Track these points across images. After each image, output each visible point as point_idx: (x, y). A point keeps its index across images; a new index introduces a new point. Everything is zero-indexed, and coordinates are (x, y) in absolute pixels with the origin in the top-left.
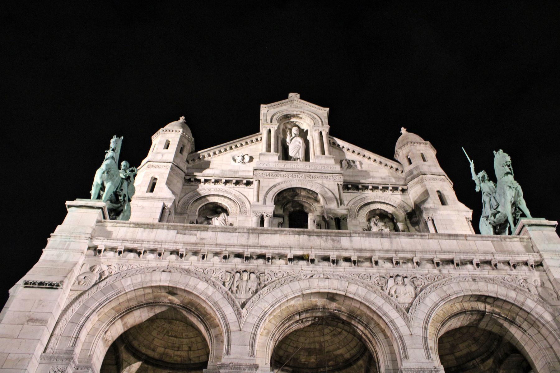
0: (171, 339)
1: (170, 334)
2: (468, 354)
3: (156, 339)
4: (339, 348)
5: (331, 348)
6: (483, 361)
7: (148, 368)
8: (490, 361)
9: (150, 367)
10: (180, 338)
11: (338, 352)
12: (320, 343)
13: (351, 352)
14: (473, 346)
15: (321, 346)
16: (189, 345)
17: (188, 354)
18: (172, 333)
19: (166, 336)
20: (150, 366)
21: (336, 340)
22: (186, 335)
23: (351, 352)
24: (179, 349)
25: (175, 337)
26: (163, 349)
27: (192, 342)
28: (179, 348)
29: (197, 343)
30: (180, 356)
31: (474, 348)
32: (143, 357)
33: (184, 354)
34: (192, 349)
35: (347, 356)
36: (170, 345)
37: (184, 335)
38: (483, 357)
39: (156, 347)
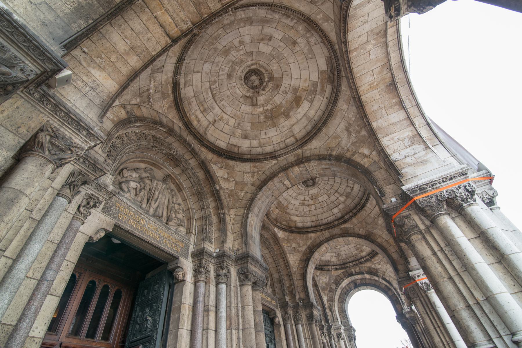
0: (208, 94)
1: (213, 87)
2: (328, 261)
3: (200, 74)
4: (297, 216)
5: (292, 212)
6: (336, 269)
7: (168, 96)
8: (340, 272)
9: (171, 98)
10: (216, 102)
11: (294, 218)
12: (289, 203)
13: (305, 223)
14: (334, 258)
15: (287, 206)
16: (217, 119)
17: (208, 127)
18: (216, 88)
19: (209, 84)
20: (172, 96)
21: (301, 208)
22: (223, 105)
23: (305, 223)
24: (204, 111)
25: (214, 96)
26: (192, 94)
27: (222, 117)
28: (205, 110)
29: (227, 123)
30: (199, 121)
31: (334, 259)
32: (178, 76)
33: (205, 123)
34: (216, 125)
35: (300, 225)
36: (201, 97)
37: (222, 102)
38: (338, 267)
39: (191, 83)
